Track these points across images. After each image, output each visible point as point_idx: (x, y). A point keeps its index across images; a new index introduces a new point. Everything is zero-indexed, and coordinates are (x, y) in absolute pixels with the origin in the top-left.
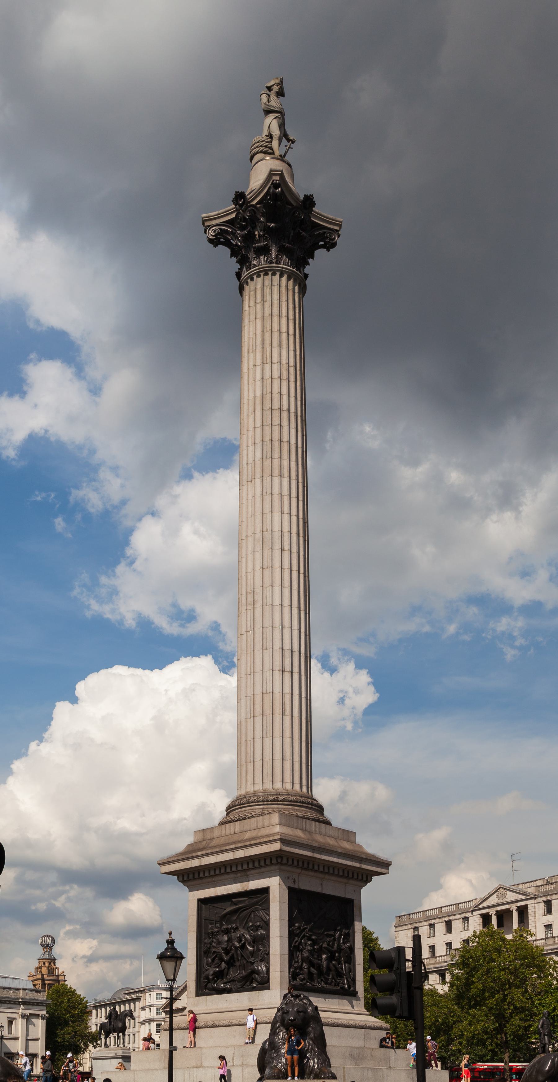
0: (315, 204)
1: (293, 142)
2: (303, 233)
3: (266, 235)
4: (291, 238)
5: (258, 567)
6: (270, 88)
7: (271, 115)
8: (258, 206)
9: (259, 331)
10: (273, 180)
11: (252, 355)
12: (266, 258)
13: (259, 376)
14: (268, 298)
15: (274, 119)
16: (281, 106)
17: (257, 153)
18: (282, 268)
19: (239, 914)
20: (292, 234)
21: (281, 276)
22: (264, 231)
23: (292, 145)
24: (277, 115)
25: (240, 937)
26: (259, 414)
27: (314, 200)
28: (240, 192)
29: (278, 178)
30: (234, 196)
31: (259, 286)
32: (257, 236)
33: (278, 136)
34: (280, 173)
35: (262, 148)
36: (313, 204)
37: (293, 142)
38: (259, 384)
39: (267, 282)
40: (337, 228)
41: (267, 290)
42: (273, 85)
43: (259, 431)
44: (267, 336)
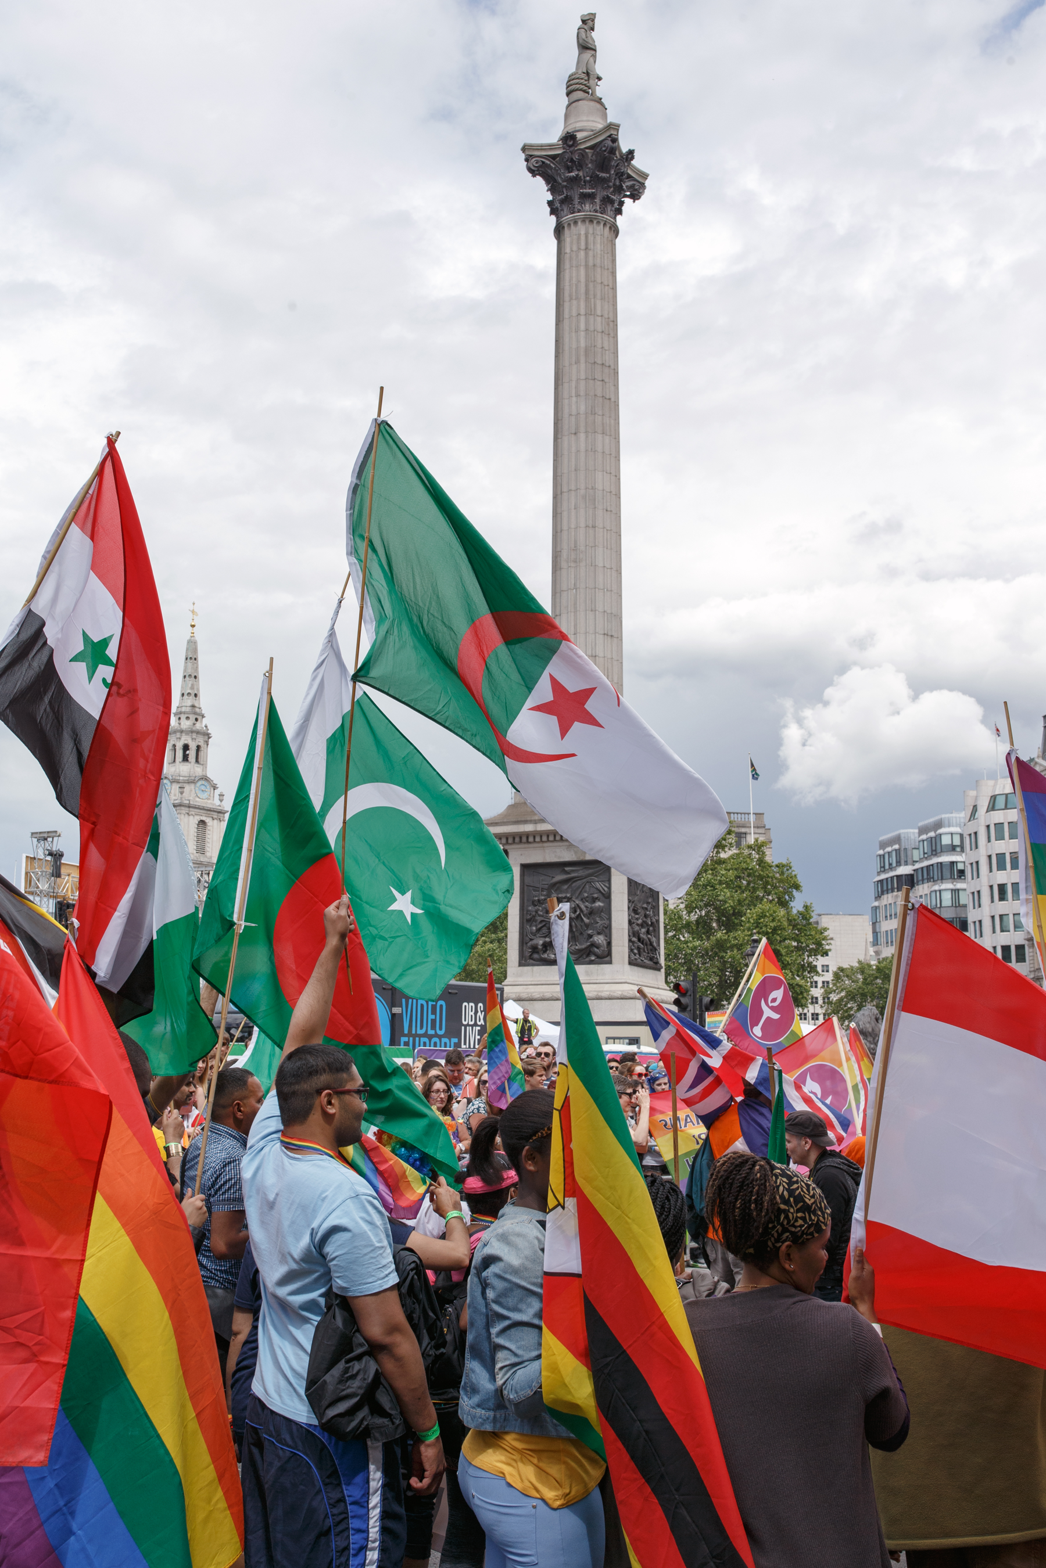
5: (583, 525)
8: (587, 151)
9: (583, 279)
11: (574, 302)
13: (582, 326)
14: (591, 246)
17: (577, 90)
19: (572, 884)
21: (605, 225)
22: (591, 177)
25: (575, 907)
26: (583, 366)
31: (583, 232)
35: (582, 86)
36: (633, 158)
38: (582, 334)
39: (591, 231)
41: (591, 238)
42: (588, 20)
43: (582, 384)
44: (591, 285)
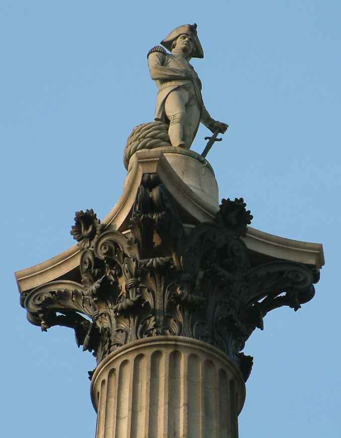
0: (251, 217)
1: (222, 128)
2: (224, 271)
3: (140, 285)
4: (198, 283)
6: (169, 44)
7: (168, 84)
10: (143, 175)
12: (141, 326)
15: (172, 91)
16: (190, 70)
18: (176, 340)
20: (201, 274)
22: (137, 276)
23: (219, 136)
24: (180, 83)
27: (247, 209)
28: (85, 212)
29: (153, 169)
30: (74, 223)
32: (124, 290)
33: (178, 116)
34: (158, 159)
37: (222, 128)
40: (312, 261)
